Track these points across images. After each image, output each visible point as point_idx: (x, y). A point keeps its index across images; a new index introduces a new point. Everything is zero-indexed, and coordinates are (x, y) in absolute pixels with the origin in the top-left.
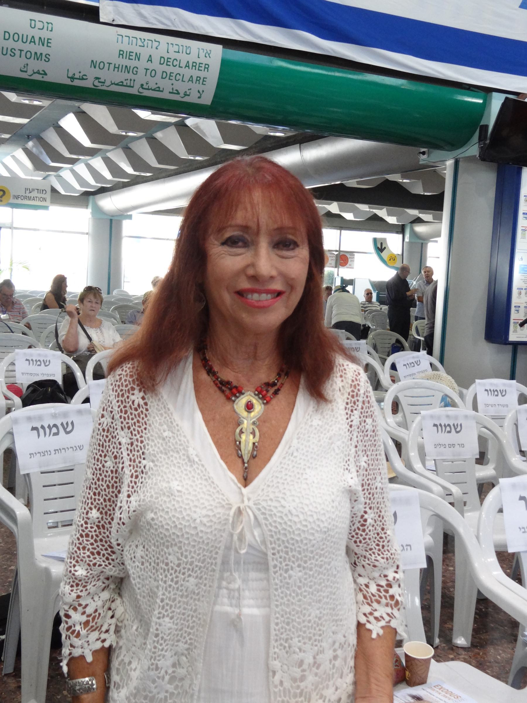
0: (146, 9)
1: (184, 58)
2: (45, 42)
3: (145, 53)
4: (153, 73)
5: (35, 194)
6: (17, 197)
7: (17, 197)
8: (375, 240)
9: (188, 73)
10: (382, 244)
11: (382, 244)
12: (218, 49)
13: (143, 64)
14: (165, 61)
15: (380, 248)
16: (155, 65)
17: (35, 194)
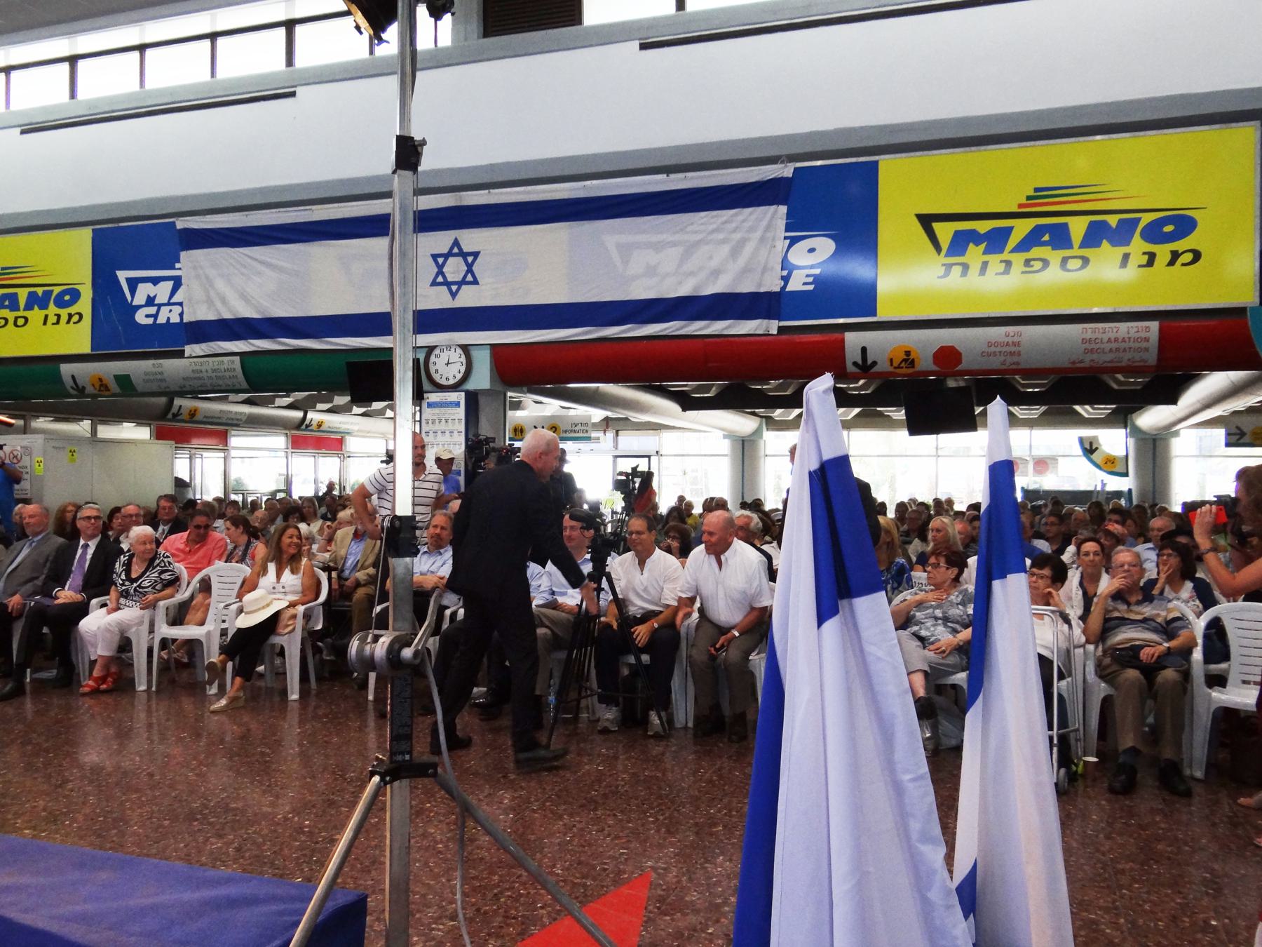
0: (203, 346)
1: (222, 367)
2: (161, 373)
3: (203, 368)
4: (210, 378)
5: (578, 428)
6: (565, 432)
7: (565, 432)
8: (1081, 440)
9: (227, 374)
10: (1091, 444)
11: (1091, 444)
12: (237, 359)
13: (205, 374)
14: (214, 371)
15: (1089, 449)
16: (210, 374)
17: (578, 428)
